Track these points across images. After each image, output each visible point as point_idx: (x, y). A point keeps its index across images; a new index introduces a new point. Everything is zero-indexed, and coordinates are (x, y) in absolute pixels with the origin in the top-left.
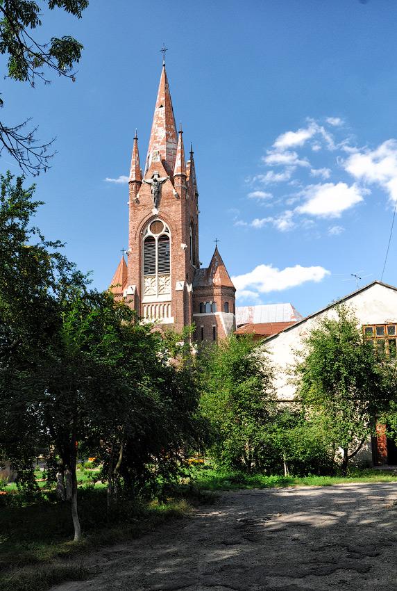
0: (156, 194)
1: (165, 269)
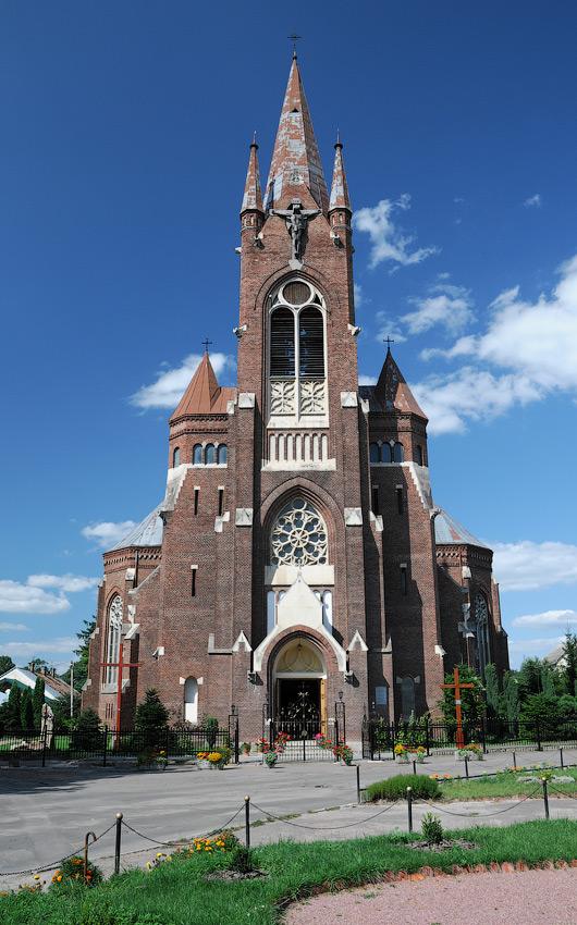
1: (313, 371)
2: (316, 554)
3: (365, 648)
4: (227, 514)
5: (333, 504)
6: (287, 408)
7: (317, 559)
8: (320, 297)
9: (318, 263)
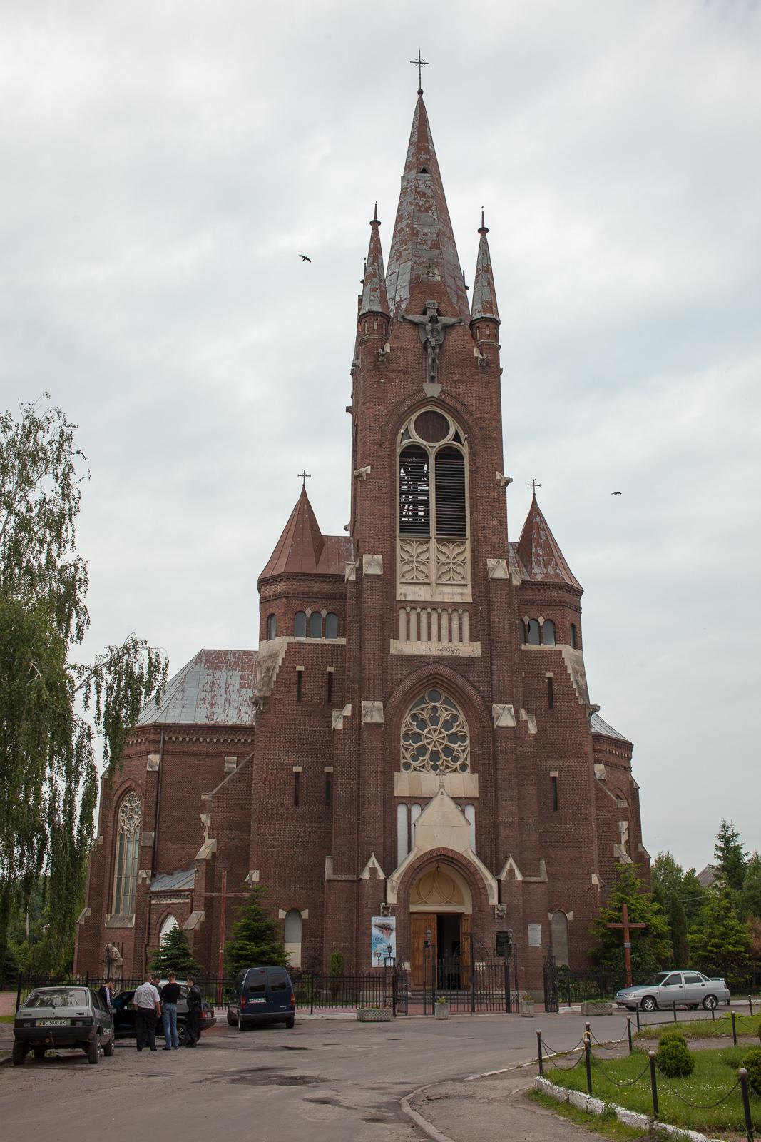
2: (455, 759)
3: (519, 877)
4: (349, 707)
5: (477, 700)
6: (420, 576)
7: (457, 765)
8: (463, 436)
9: (461, 389)
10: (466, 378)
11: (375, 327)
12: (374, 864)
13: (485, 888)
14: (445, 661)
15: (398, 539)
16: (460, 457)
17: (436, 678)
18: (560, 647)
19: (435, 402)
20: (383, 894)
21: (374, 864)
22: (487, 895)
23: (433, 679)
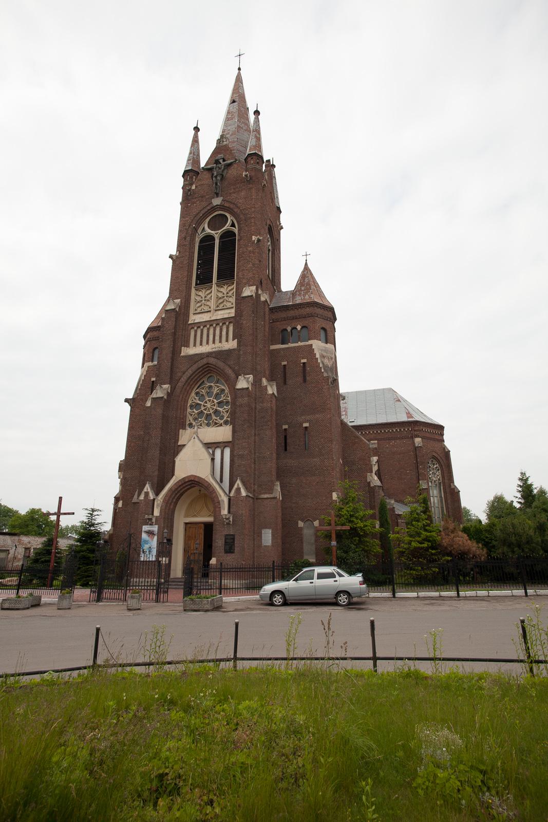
0: (219, 178)
1: (227, 275)
3: (244, 493)
10: (237, 190)
11: (188, 178)
12: (147, 489)
13: (219, 502)
14: (214, 355)
15: (193, 290)
16: (235, 235)
17: (208, 367)
18: (310, 342)
19: (220, 208)
20: (151, 510)
21: (147, 489)
22: (220, 507)
23: (207, 367)
